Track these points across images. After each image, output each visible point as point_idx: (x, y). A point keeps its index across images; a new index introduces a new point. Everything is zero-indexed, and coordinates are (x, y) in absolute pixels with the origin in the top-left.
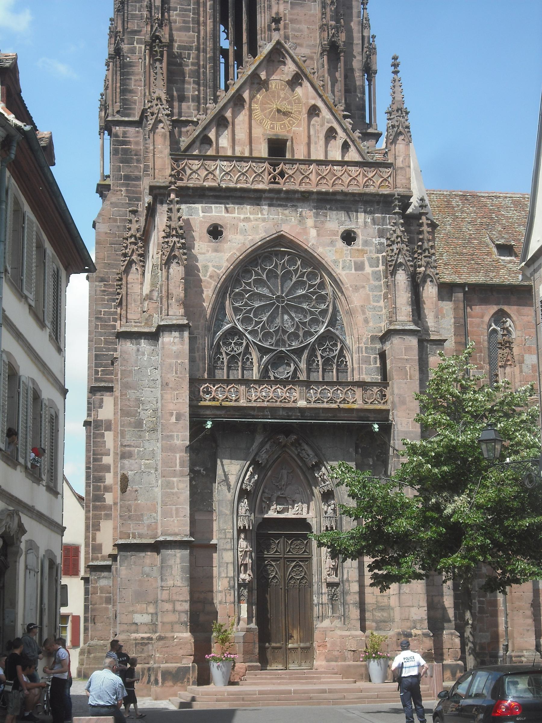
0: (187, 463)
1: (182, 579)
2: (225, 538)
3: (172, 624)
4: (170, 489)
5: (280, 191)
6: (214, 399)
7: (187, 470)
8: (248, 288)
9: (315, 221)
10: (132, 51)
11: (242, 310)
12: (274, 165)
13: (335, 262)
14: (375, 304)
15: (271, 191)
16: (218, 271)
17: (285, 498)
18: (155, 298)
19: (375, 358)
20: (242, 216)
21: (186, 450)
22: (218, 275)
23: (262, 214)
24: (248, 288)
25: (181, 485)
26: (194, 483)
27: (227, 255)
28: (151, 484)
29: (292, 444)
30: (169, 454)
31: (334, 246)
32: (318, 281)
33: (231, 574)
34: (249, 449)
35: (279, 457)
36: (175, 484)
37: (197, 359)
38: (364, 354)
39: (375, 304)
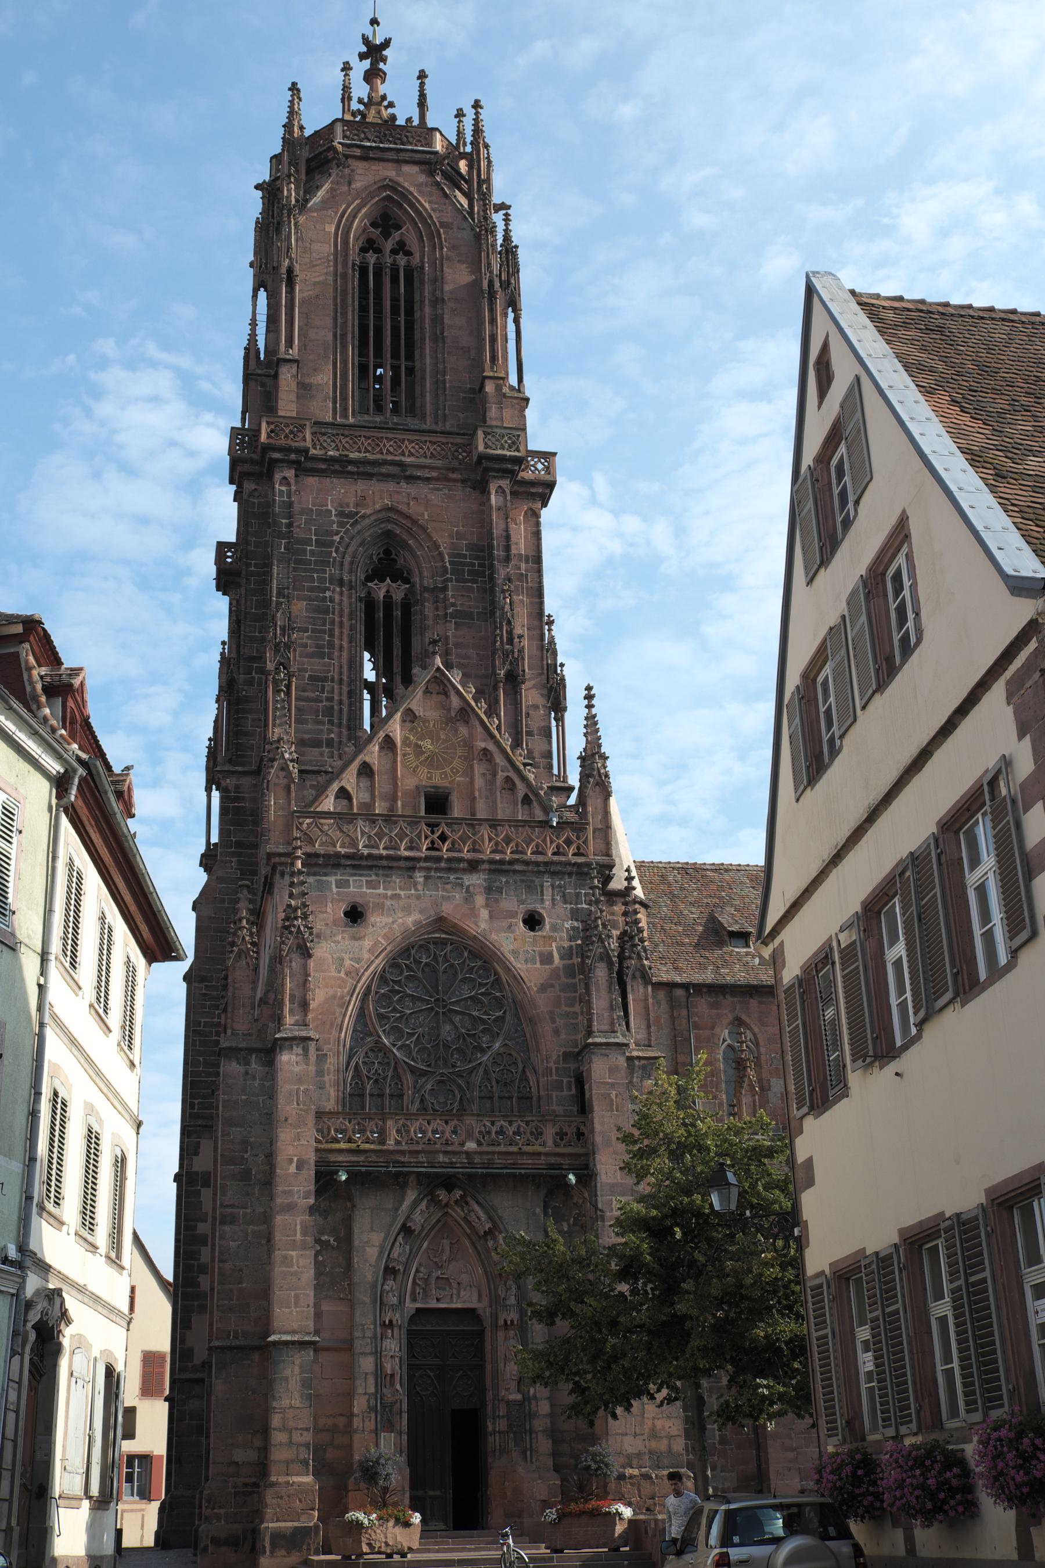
1: (302, 1397)
2: (364, 1337)
3: (288, 1463)
4: (287, 1267)
5: (439, 859)
7: (310, 1240)
8: (397, 988)
9: (487, 899)
11: (388, 1018)
12: (433, 826)
13: (515, 953)
14: (568, 1009)
15: (427, 859)
16: (356, 965)
17: (447, 1279)
18: (271, 1002)
19: (569, 1083)
20: (389, 893)
22: (357, 971)
23: (416, 890)
24: (397, 988)
25: (303, 1262)
26: (320, 1258)
27: (368, 943)
29: (457, 1202)
31: (513, 932)
32: (492, 978)
33: (371, 1389)
34: (397, 1210)
35: (438, 1221)
37: (327, 1085)
38: (555, 1077)
39: (568, 1009)
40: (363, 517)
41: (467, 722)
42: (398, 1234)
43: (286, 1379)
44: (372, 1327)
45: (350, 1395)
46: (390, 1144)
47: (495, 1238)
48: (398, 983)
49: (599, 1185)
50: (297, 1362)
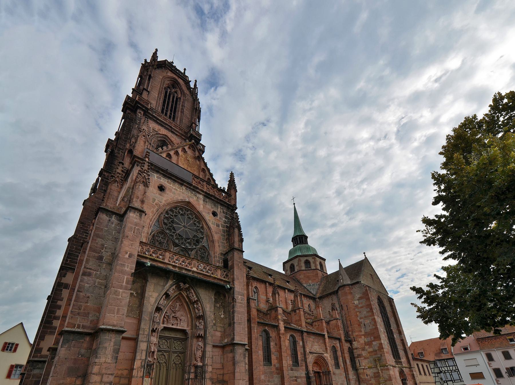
0: (131, 283)
1: (112, 357)
2: (144, 334)
4: (116, 295)
6: (151, 255)
7: (130, 286)
10: (119, 153)
17: (176, 318)
20: (174, 187)
21: (131, 275)
27: (165, 199)
28: (100, 295)
30: (120, 275)
36: (120, 293)
40: (159, 134)
41: (199, 161)
42: (163, 296)
43: (106, 348)
44: (148, 330)
45: (133, 360)
46: (166, 261)
47: (197, 304)
48: (172, 216)
49: (235, 291)
50: (113, 340)
